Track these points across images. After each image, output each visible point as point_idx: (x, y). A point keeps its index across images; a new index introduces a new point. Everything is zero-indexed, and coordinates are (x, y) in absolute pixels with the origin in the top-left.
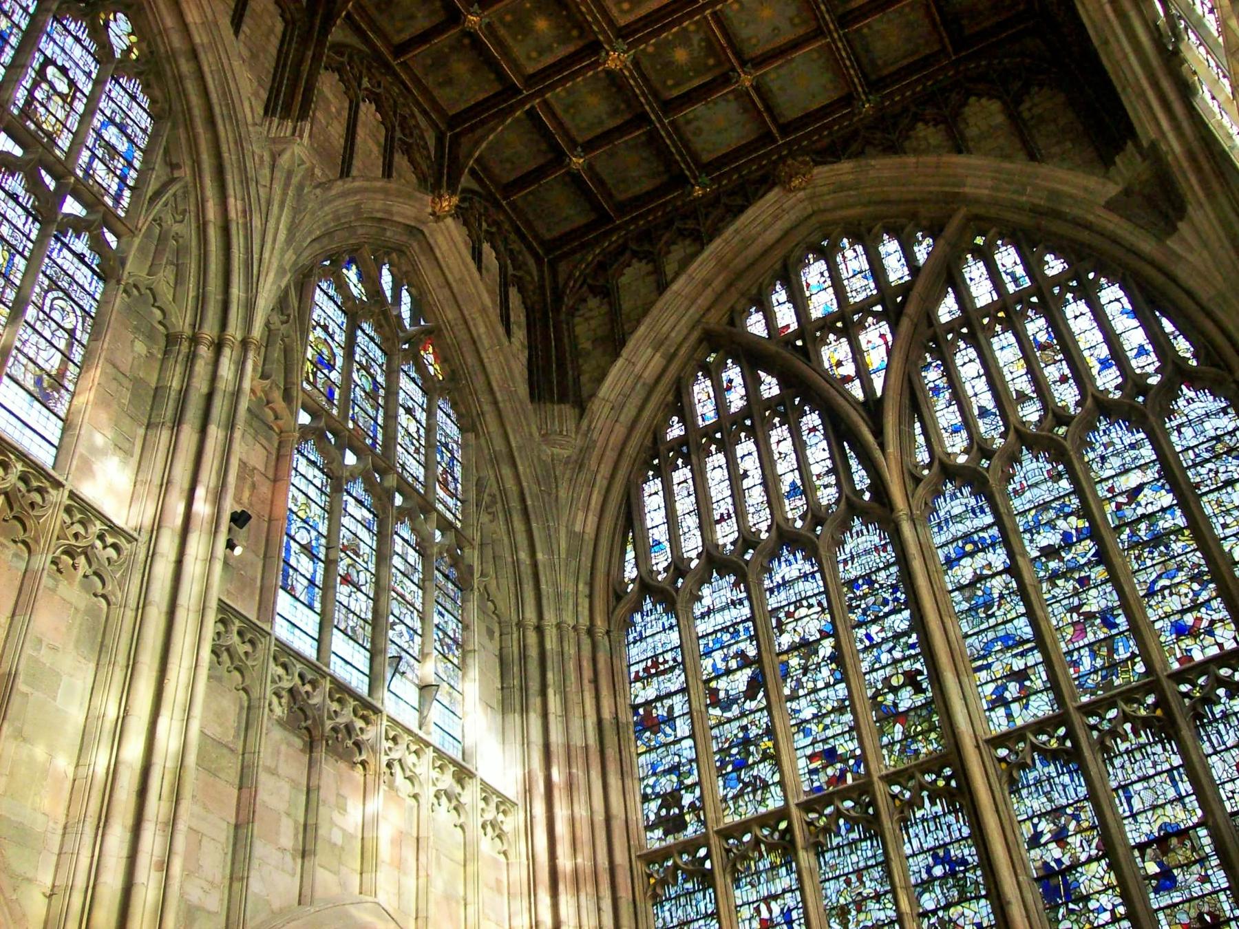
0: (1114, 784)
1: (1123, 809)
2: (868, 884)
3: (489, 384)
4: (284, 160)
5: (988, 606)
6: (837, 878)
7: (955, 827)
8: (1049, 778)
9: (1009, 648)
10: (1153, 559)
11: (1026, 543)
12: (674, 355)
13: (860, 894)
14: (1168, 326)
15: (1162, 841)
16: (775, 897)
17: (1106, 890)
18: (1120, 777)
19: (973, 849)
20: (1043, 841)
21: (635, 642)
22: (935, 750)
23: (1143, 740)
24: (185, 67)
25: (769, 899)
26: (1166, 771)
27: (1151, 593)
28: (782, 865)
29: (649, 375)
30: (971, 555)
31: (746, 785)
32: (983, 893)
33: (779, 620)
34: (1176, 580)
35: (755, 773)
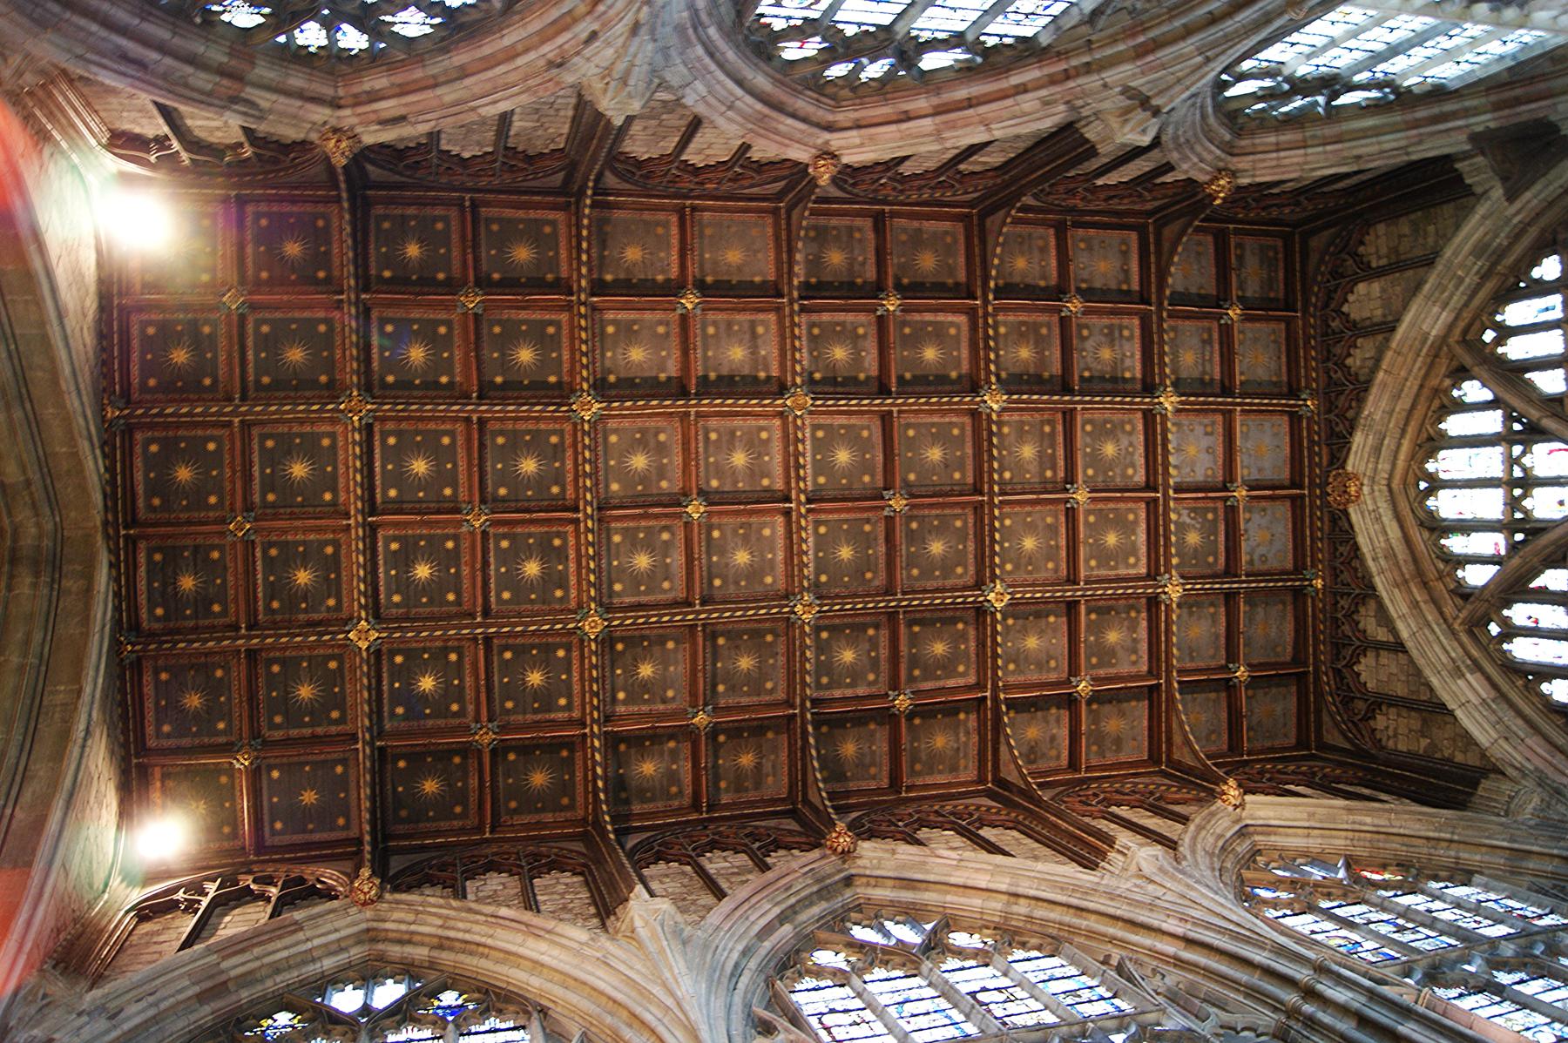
3: (1428, 839)
4: (1148, 869)
12: (1474, 661)
24: (1022, 908)
29: (1485, 691)
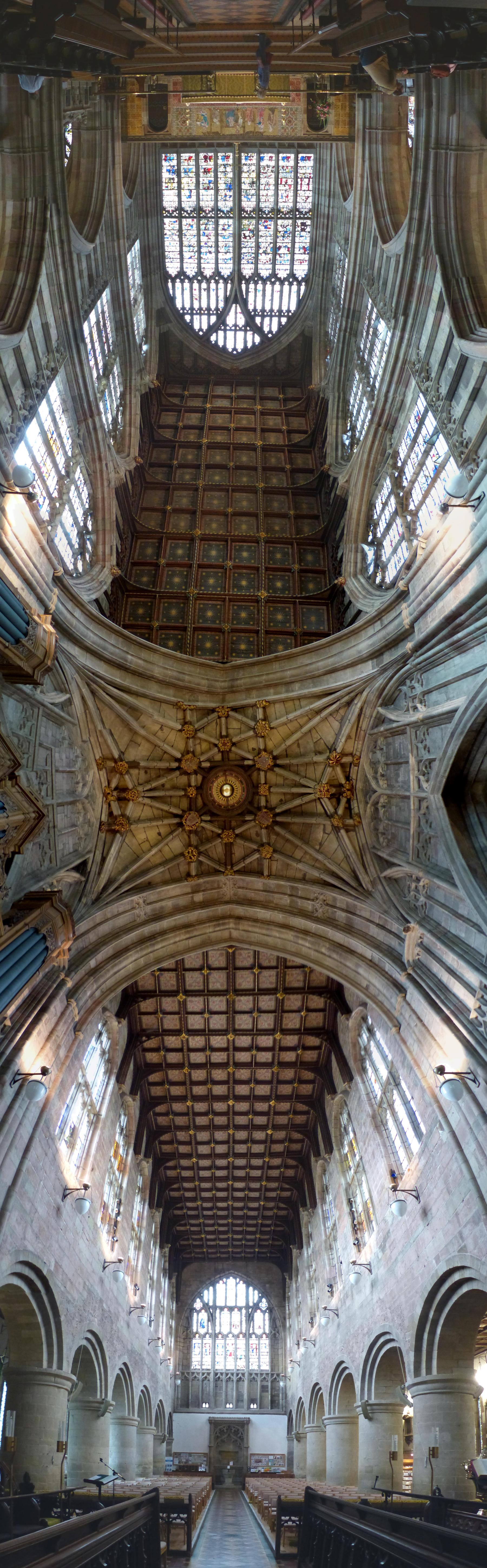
15: (208, 188)
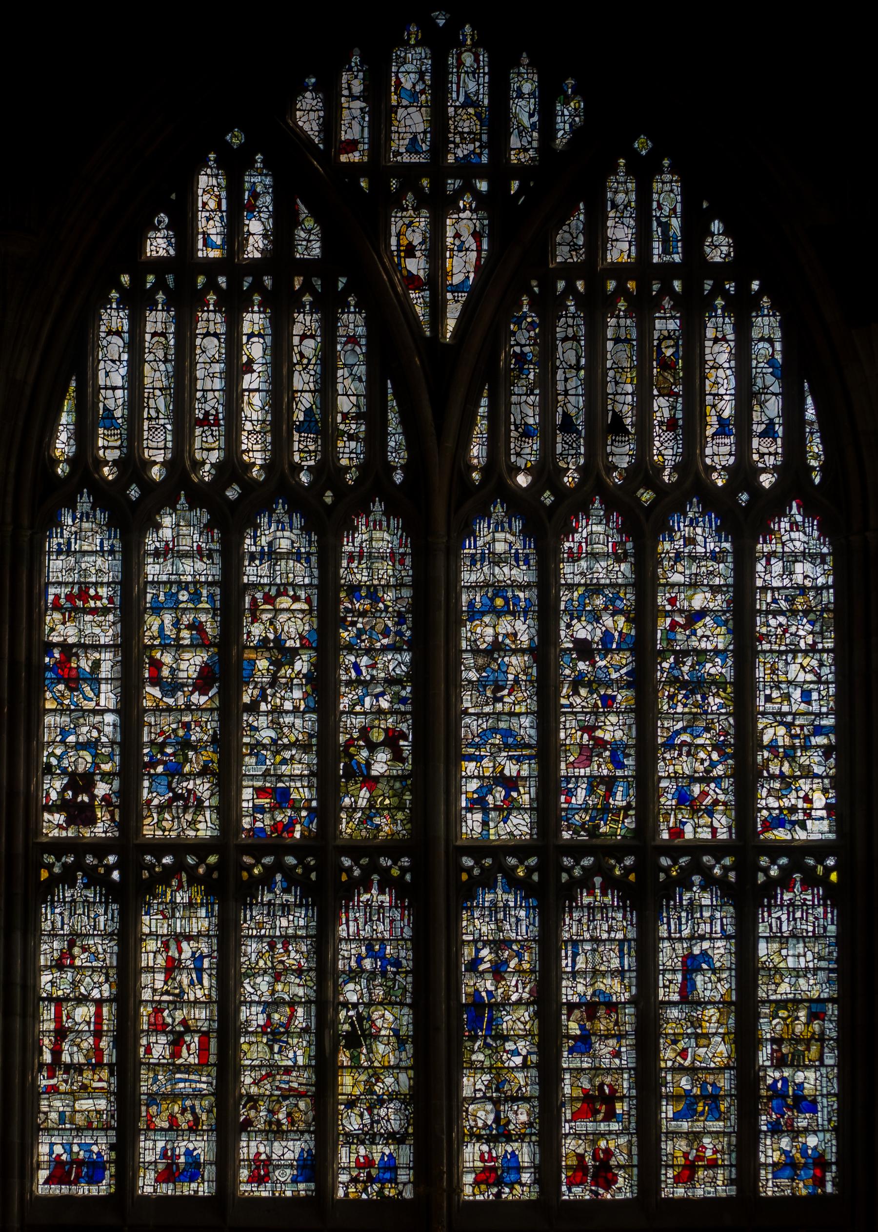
0: (566, 936)
1: (566, 964)
2: (293, 954)
5: (498, 688)
6: (261, 938)
7: (398, 924)
8: (506, 906)
9: (507, 746)
10: (685, 705)
11: (563, 626)
13: (282, 962)
14: (810, 413)
16: (189, 938)
17: (526, 1035)
18: (574, 930)
19: (410, 953)
20: (482, 968)
21: (59, 552)
22: (398, 833)
23: (608, 900)
25: (180, 938)
26: (619, 940)
27: (669, 745)
28: (202, 905)
30: (499, 614)
31: (177, 797)
32: (408, 1001)
33: (254, 600)
34: (699, 741)
35: (190, 787)
